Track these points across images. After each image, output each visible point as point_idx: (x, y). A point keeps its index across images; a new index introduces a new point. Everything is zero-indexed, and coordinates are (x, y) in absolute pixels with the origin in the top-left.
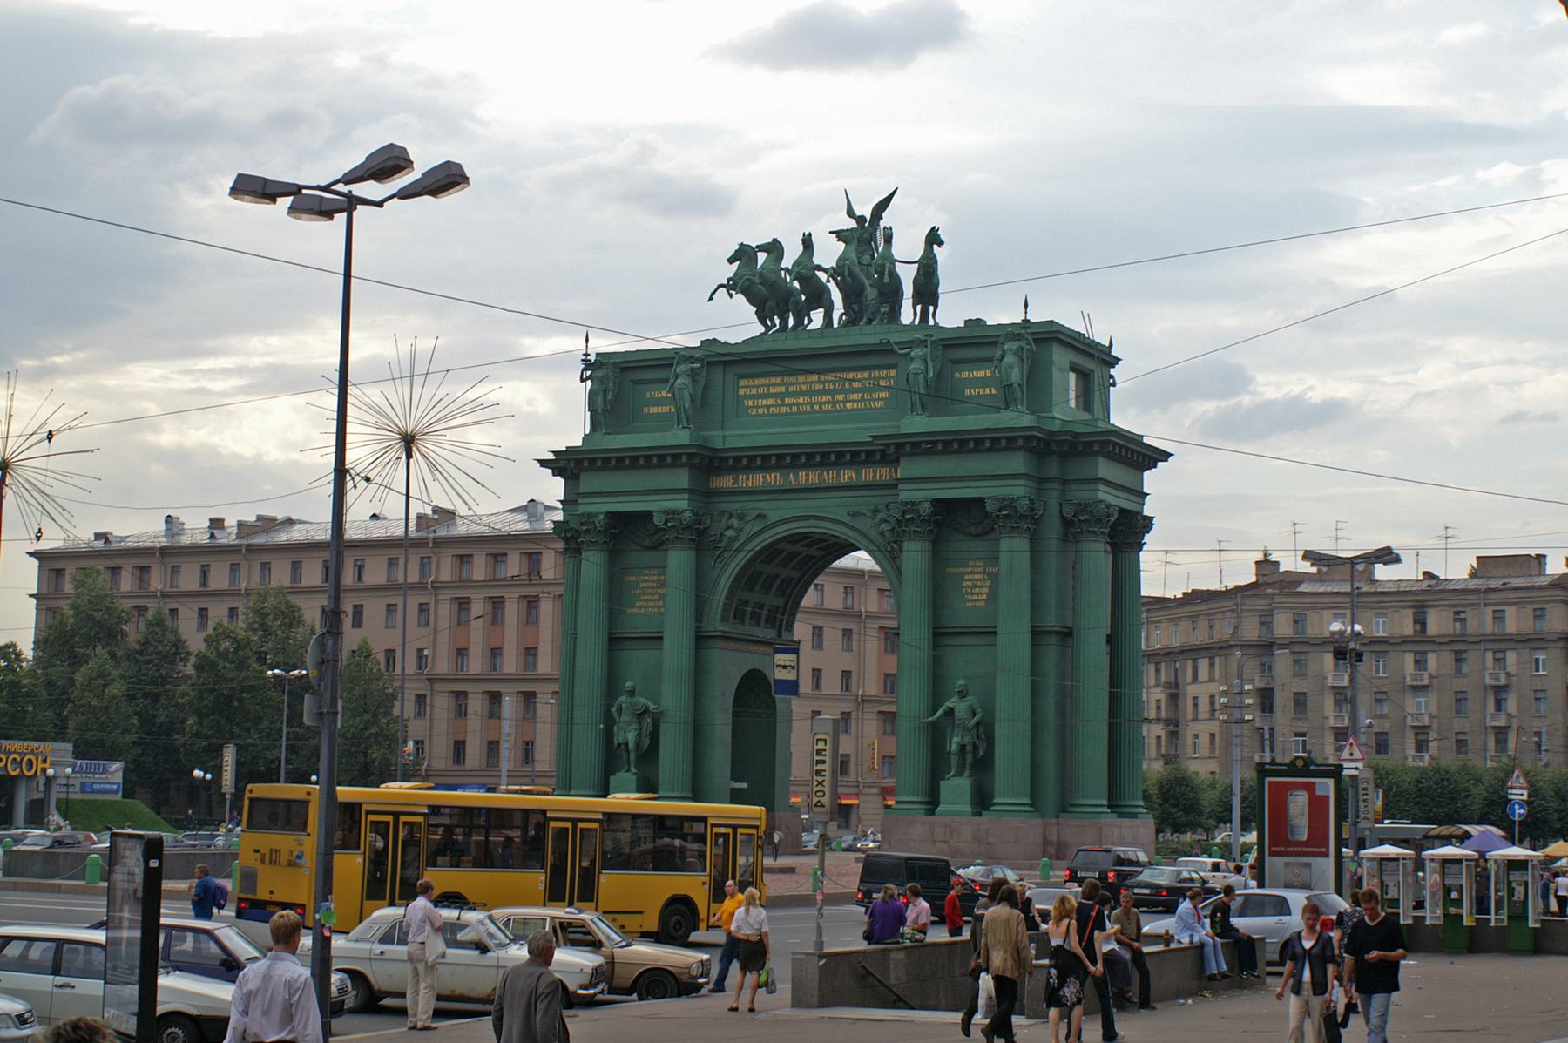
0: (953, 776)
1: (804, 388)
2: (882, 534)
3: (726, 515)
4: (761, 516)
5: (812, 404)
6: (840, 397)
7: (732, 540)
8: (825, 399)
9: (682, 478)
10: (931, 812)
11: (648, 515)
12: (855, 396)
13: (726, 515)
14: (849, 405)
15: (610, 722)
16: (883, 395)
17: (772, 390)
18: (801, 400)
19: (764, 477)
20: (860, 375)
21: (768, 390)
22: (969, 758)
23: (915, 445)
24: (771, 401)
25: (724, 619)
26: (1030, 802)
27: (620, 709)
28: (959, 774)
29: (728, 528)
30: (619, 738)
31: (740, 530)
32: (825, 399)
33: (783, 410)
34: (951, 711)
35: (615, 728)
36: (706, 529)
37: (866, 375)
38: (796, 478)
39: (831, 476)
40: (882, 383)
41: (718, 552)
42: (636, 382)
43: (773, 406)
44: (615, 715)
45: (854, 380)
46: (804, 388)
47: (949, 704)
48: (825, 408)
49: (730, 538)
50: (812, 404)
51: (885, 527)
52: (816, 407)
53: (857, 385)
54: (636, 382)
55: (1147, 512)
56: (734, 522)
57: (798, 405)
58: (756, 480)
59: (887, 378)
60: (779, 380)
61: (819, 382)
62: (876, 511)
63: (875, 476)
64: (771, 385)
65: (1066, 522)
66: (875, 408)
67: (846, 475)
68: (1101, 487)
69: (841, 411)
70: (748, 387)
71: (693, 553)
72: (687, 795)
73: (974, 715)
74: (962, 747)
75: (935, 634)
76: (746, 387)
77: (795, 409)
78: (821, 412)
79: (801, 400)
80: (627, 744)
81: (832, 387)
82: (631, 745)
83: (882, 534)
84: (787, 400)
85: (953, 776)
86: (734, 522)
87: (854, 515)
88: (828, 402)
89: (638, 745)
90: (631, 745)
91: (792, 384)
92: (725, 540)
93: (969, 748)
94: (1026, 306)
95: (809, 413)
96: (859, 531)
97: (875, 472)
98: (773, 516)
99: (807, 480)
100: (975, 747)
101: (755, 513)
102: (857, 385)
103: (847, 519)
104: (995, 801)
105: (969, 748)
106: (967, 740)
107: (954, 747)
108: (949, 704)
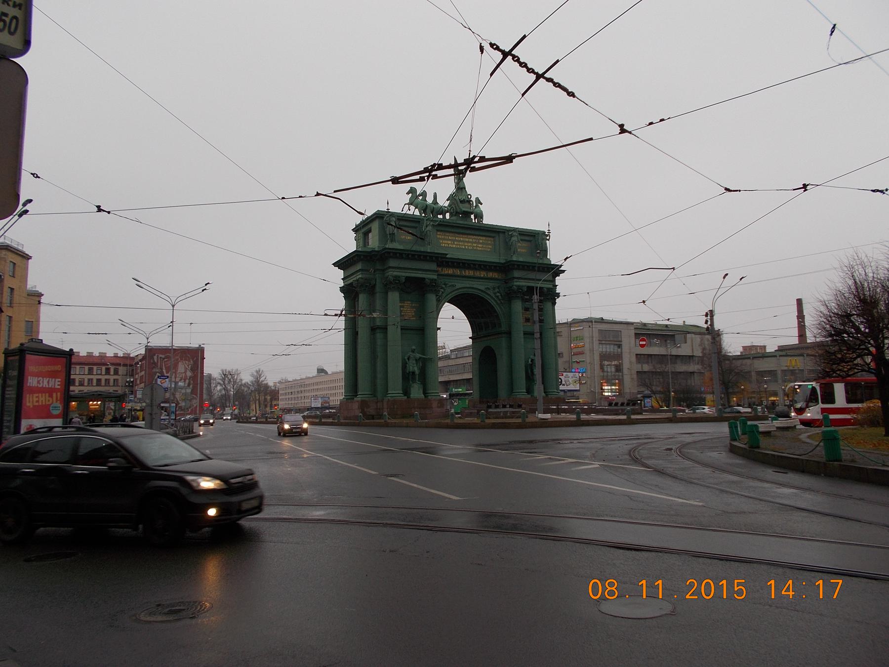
1: (461, 239)
2: (498, 297)
5: (465, 246)
6: (475, 245)
8: (469, 244)
9: (433, 266)
11: (424, 279)
12: (480, 246)
14: (478, 248)
16: (490, 247)
17: (450, 238)
18: (461, 243)
20: (482, 238)
24: (449, 242)
29: (441, 288)
32: (469, 244)
33: (454, 246)
37: (484, 238)
38: (465, 273)
39: (477, 274)
40: (489, 242)
45: (481, 239)
48: (470, 248)
51: (498, 294)
52: (467, 247)
53: (481, 241)
57: (460, 245)
58: (450, 271)
59: (491, 240)
60: (453, 234)
67: (483, 274)
69: (475, 250)
70: (440, 235)
76: (440, 236)
79: (461, 243)
80: (413, 373)
83: (498, 297)
84: (455, 243)
90: (417, 372)
91: (457, 237)
96: (489, 295)
98: (459, 286)
99: (469, 273)
101: (450, 284)
102: (481, 241)
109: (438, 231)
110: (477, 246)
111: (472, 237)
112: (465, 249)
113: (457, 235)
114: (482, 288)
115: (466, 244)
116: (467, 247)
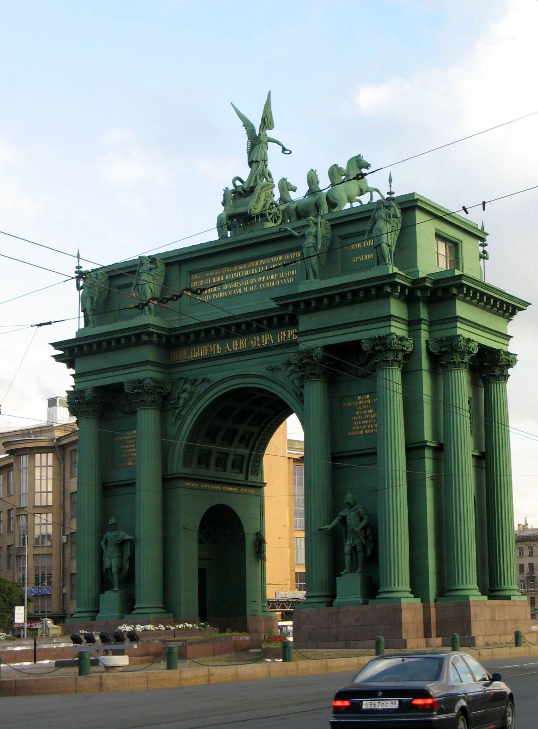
0: (346, 573)
1: (236, 275)
3: (183, 381)
4: (208, 381)
6: (262, 279)
7: (186, 401)
8: (251, 282)
10: (330, 604)
13: (183, 381)
14: (269, 285)
15: (101, 554)
18: (235, 285)
19: (208, 348)
21: (211, 280)
22: (360, 555)
23: (307, 303)
24: (214, 290)
25: (186, 463)
26: (410, 590)
27: (106, 543)
28: (353, 570)
30: (107, 563)
31: (193, 392)
34: (344, 520)
35: (104, 556)
36: (170, 394)
41: (177, 411)
42: (120, 287)
43: (214, 293)
44: (103, 547)
46: (236, 275)
47: (342, 513)
48: (252, 289)
49: (185, 399)
50: (242, 287)
54: (120, 287)
55: (511, 349)
56: (188, 386)
57: (232, 289)
58: (202, 352)
61: (246, 269)
62: (289, 364)
63: (286, 338)
64: (214, 276)
65: (433, 358)
66: (288, 284)
67: (267, 338)
68: (459, 325)
69: (263, 289)
70: (196, 280)
71: (158, 413)
72: (159, 606)
73: (362, 519)
74: (354, 548)
75: (335, 457)
77: (230, 293)
78: (249, 292)
81: (256, 272)
82: (114, 570)
84: (225, 287)
85: (346, 573)
86: (188, 386)
87: (272, 369)
88: (252, 284)
89: (120, 570)
90: (114, 570)
91: (228, 273)
92: (181, 402)
93: (359, 548)
94: (390, 180)
95: (240, 294)
97: (287, 334)
100: (364, 548)
101: (201, 378)
103: (267, 374)
104: (380, 591)
105: (359, 548)
106: (357, 542)
107: (347, 549)
108: (342, 513)
109: (191, 273)
110: (265, 282)
111: (257, 263)
112: (243, 293)
113: (227, 270)
114: (261, 370)
115: (245, 283)
116: (245, 289)
